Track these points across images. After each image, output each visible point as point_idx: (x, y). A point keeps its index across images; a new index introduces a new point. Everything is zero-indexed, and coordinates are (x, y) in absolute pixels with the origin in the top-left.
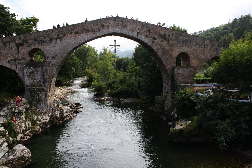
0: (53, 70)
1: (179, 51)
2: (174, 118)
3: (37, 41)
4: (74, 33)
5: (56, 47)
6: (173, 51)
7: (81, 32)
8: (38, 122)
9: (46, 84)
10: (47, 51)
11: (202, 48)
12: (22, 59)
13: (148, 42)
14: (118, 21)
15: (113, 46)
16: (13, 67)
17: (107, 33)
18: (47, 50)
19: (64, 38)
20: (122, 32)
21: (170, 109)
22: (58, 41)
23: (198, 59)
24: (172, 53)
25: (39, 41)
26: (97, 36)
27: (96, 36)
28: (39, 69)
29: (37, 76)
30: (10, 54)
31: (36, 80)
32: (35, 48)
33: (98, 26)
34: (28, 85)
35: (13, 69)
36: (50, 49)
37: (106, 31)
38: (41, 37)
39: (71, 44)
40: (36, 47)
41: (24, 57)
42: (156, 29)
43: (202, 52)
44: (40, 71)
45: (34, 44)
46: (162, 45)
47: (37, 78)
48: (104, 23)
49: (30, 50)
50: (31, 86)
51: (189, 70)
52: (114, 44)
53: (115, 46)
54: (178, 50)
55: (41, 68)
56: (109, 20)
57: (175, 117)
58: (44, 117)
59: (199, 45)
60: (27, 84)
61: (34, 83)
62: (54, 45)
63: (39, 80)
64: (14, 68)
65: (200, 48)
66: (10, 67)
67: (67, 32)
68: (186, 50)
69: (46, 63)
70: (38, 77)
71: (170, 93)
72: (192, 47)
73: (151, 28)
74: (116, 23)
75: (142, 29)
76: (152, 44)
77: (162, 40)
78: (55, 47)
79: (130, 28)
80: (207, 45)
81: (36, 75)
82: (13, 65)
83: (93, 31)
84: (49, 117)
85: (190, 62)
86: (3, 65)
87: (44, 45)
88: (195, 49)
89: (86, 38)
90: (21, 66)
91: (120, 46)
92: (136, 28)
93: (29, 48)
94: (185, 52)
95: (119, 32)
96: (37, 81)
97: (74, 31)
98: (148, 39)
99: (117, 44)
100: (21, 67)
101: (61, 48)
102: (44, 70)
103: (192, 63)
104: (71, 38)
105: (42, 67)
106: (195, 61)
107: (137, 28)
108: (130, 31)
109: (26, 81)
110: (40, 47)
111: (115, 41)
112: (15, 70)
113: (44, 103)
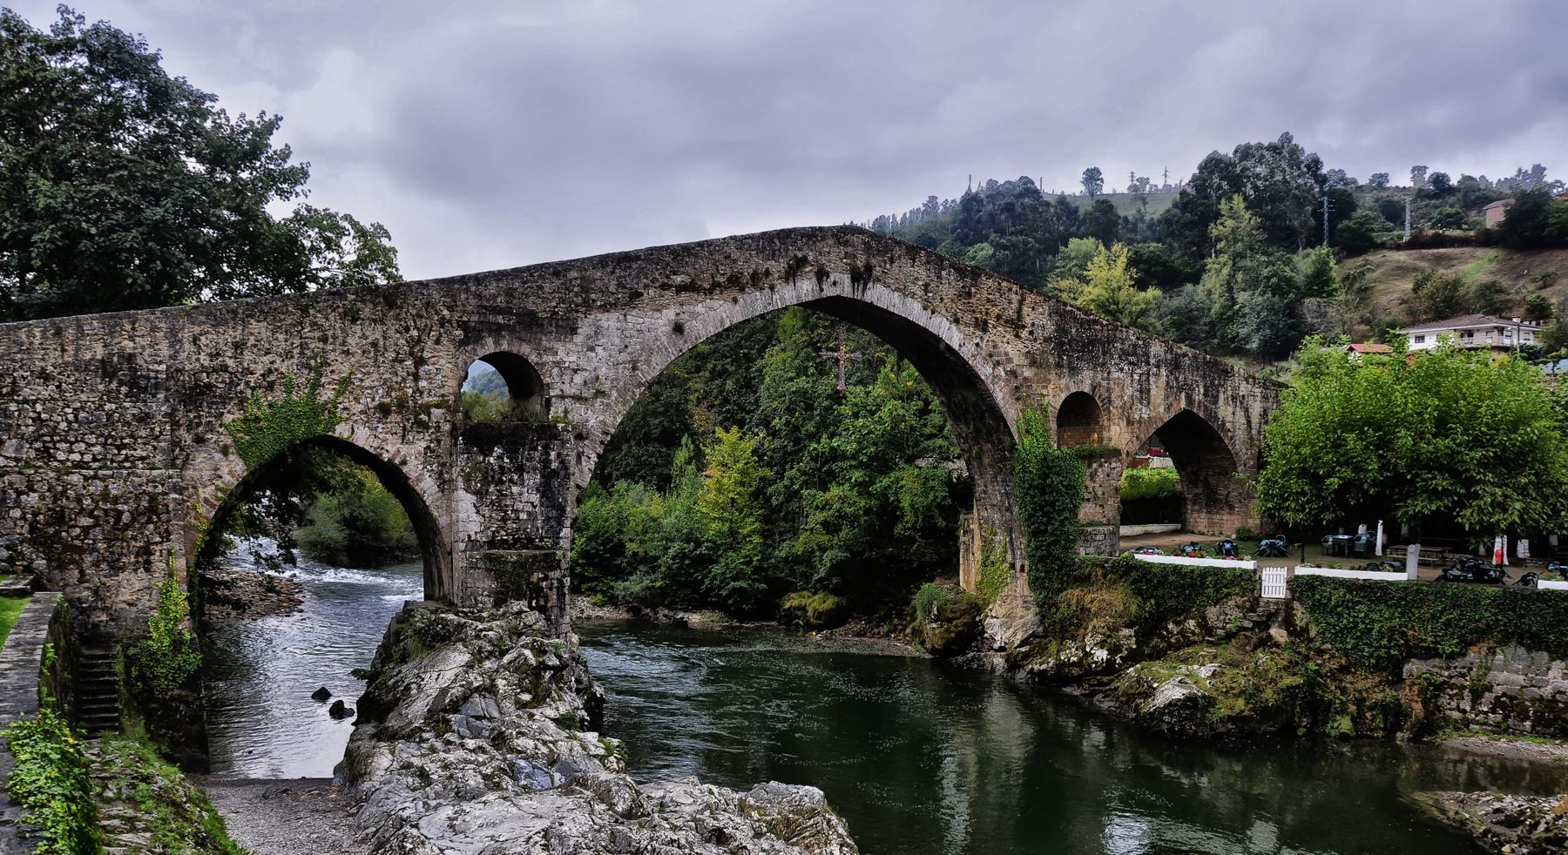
0: (584, 463)
2: (1089, 665)
4: (681, 289)
7: (707, 286)
10: (555, 371)
11: (1141, 375)
12: (437, 406)
14: (853, 246)
18: (557, 364)
21: (1033, 635)
22: (610, 321)
23: (1130, 422)
27: (765, 307)
28: (530, 459)
29: (521, 494)
30: (375, 376)
35: (386, 457)
36: (571, 359)
38: (527, 296)
40: (505, 347)
41: (443, 396)
43: (1141, 392)
44: (535, 469)
46: (1010, 360)
47: (519, 506)
48: (800, 250)
50: (492, 543)
54: (1063, 381)
55: (537, 454)
57: (1096, 663)
59: (1131, 363)
60: (469, 536)
61: (502, 528)
65: (1136, 377)
66: (375, 445)
68: (1088, 382)
69: (565, 429)
78: (592, 349)
80: (1158, 367)
83: (757, 280)
85: (1100, 433)
86: (337, 435)
92: (917, 279)
93: (469, 348)
94: (1086, 391)
96: (518, 518)
97: (678, 279)
100: (428, 448)
101: (624, 357)
102: (554, 465)
104: (665, 311)
105: (547, 449)
108: (896, 294)
110: (525, 349)
112: (397, 461)
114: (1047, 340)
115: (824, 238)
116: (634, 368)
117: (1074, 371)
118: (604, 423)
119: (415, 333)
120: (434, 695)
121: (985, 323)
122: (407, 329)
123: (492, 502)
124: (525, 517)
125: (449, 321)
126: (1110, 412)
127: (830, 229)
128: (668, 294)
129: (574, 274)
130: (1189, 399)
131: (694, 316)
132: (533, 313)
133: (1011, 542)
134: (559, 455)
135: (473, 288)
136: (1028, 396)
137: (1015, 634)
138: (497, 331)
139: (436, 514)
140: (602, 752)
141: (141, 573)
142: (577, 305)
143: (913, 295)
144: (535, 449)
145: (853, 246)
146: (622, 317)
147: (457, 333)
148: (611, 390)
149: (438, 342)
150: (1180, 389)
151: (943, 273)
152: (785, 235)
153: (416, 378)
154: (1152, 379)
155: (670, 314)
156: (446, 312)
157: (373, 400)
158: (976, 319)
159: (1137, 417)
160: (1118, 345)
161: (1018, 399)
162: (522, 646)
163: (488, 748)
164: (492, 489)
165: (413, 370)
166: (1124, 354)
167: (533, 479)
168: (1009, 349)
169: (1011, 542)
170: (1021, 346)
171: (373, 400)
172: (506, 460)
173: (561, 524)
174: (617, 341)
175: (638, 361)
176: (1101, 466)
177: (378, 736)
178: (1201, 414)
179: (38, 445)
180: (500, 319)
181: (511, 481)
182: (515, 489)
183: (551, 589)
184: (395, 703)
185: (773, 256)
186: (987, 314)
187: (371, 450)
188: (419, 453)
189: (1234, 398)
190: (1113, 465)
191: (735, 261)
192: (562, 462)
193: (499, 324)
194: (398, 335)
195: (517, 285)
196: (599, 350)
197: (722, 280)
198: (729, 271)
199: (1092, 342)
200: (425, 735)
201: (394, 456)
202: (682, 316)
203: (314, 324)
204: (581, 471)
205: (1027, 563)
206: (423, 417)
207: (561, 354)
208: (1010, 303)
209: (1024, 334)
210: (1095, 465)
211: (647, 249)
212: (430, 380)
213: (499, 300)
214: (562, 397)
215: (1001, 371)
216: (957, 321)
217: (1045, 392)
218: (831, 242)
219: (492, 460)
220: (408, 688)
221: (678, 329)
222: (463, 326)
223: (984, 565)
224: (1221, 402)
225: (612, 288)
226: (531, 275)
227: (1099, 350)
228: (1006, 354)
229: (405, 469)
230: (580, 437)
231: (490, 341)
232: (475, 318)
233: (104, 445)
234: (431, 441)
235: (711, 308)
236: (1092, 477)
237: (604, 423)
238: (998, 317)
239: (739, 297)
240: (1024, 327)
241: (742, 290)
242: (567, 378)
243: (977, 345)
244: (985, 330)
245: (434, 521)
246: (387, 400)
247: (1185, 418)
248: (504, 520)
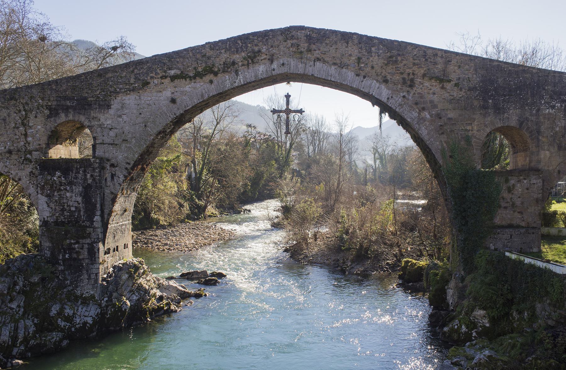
0: (116, 180)
4: (173, 78)
7: (191, 74)
8: (62, 323)
9: (95, 219)
10: (99, 129)
12: (36, 150)
13: (388, 98)
14: (298, 39)
15: (281, 114)
17: (265, 76)
19: (145, 91)
20: (310, 71)
22: (130, 100)
25: (77, 100)
26: (236, 85)
27: (232, 84)
32: (67, 120)
33: (238, 56)
34: (47, 221)
37: (261, 69)
39: (164, 108)
40: (71, 117)
41: (40, 145)
42: (415, 55)
46: (435, 106)
48: (256, 45)
49: (56, 124)
50: (56, 223)
51: (525, 181)
52: (284, 108)
53: (288, 111)
56: (271, 37)
58: (81, 310)
60: (44, 219)
62: (119, 113)
63: (76, 207)
67: (151, 75)
72: (538, 110)
73: (399, 55)
74: (292, 44)
75: (371, 59)
76: (400, 105)
77: (434, 89)
78: (120, 116)
79: (334, 57)
82: (12, 166)
84: (99, 310)
88: (549, 114)
89: (204, 91)
91: (301, 111)
92: (350, 55)
93: (52, 119)
95: (301, 71)
96: (70, 210)
97: (172, 72)
98: (388, 89)
99: (293, 107)
100: (32, 172)
102: (90, 181)
106: (547, 152)
107: (354, 58)
108: (333, 67)
109: (43, 208)
111: (288, 97)
113: (87, 271)
114: (470, 89)
115: (274, 36)
116: (145, 126)
117: (498, 110)
118: (127, 158)
119: (24, 113)
121: (412, 80)
122: (20, 111)
123: (56, 201)
124: (74, 209)
125: (42, 106)
126: (538, 140)
127: (280, 30)
128: (167, 81)
129: (110, 75)
131: (183, 93)
134: (92, 176)
135: (54, 87)
136: (452, 131)
138: (66, 109)
142: (110, 93)
143: (347, 66)
144: (79, 173)
145: (298, 39)
146: (138, 98)
147: (46, 112)
148: (132, 138)
149: (36, 117)
151: (373, 49)
152: (245, 38)
153: (26, 135)
155: (168, 94)
156: (40, 101)
157: (5, 148)
158: (404, 79)
161: (443, 133)
164: (56, 194)
165: (24, 132)
168: (435, 98)
170: (447, 95)
171: (5, 148)
173: (94, 215)
174: (135, 111)
175: (148, 122)
176: (519, 181)
180: (68, 103)
181: (66, 189)
182: (68, 194)
183: (82, 249)
185: (237, 51)
186: (413, 74)
188: (27, 175)
190: (535, 181)
191: (209, 58)
192: (94, 180)
193: (67, 106)
194: (15, 115)
195: (77, 84)
196: (124, 117)
197: (200, 69)
198: (204, 65)
201: (15, 176)
202: (176, 94)
204: (114, 185)
206: (28, 156)
207: (102, 120)
208: (435, 63)
209: (448, 86)
210: (512, 182)
211: (153, 56)
212: (33, 137)
213: (67, 93)
214: (103, 143)
215: (426, 115)
216: (386, 81)
217: (469, 128)
218: (281, 38)
219: (55, 178)
221: (173, 101)
222: (49, 108)
225: (132, 81)
226: (86, 78)
228: (431, 102)
230: (112, 165)
231: (63, 115)
235: (195, 88)
236: (510, 190)
237: (127, 158)
238: (424, 76)
239: (215, 79)
240: (449, 81)
241: (216, 74)
242: (104, 133)
243: (404, 97)
244: (411, 86)
246: (12, 148)
248: (63, 210)
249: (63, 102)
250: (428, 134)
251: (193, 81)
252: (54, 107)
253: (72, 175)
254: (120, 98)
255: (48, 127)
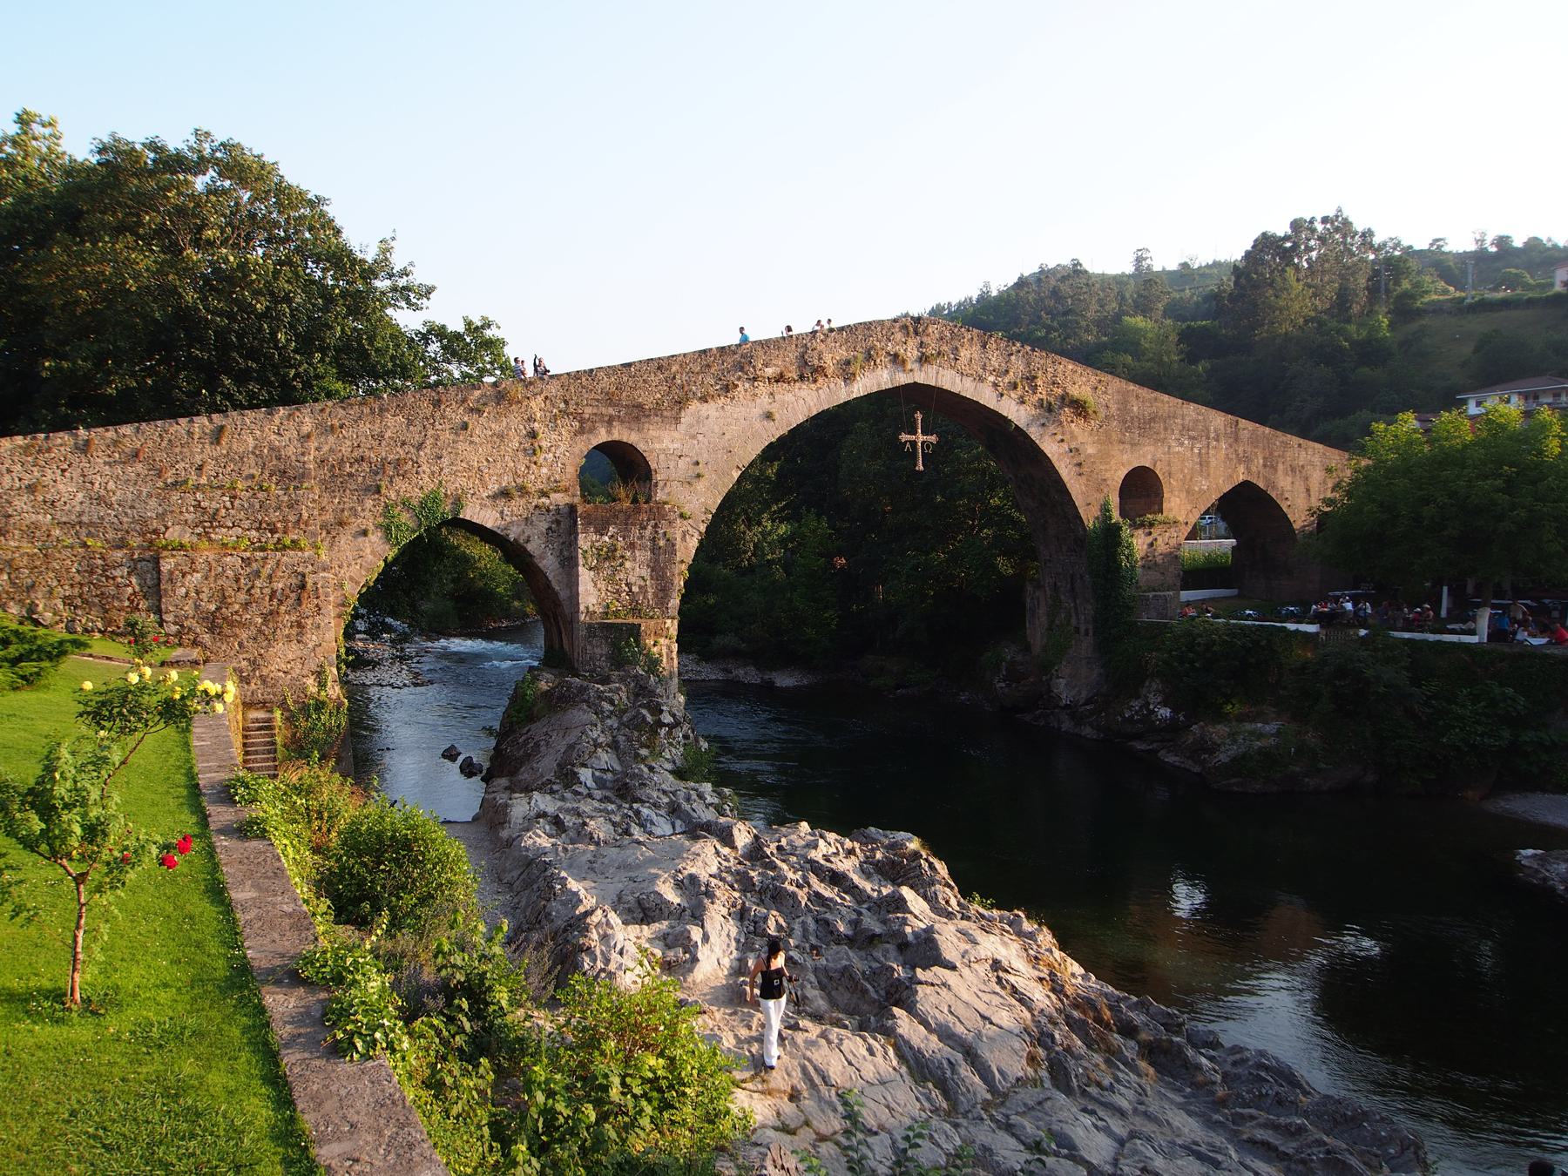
1: (1130, 463)
3: (622, 406)
5: (700, 437)
6: (1109, 463)
16: (514, 529)
17: (891, 386)
22: (709, 409)
24: (1106, 470)
31: (627, 585)
35: (512, 537)
36: (675, 446)
40: (616, 436)
45: (607, 419)
47: (632, 579)
54: (1125, 457)
57: (1159, 720)
59: (1191, 438)
60: (587, 608)
63: (640, 587)
64: (520, 529)
65: (1196, 451)
68: (1149, 457)
70: (636, 570)
71: (1087, 630)
78: (693, 437)
81: (628, 564)
86: (468, 518)
87: (651, 428)
88: (1178, 453)
90: (553, 523)
96: (631, 591)
97: (770, 371)
100: (550, 528)
103: (1171, 510)
105: (656, 526)
120: (562, 751)
130: (1248, 468)
132: (640, 406)
133: (1076, 608)
137: (1079, 693)
138: (610, 421)
139: (557, 588)
140: (716, 801)
141: (294, 645)
150: (1240, 461)
154: (1212, 452)
159: (1197, 489)
160: (1178, 421)
162: (640, 706)
163: (614, 798)
166: (1184, 429)
167: (643, 555)
169: (1076, 608)
172: (620, 539)
177: (511, 789)
178: (1261, 485)
179: (199, 530)
184: (528, 757)
187: (499, 532)
189: (1293, 469)
196: (700, 437)
199: (1153, 420)
200: (555, 787)
201: (519, 535)
203: (443, 417)
205: (1091, 627)
217: (1108, 467)
220: (537, 745)
221: (769, 416)
223: (1050, 629)
224: (1280, 472)
227: (1159, 426)
229: (529, 547)
231: (603, 431)
232: (588, 410)
233: (258, 529)
234: (553, 523)
245: (556, 594)
247: (1246, 485)
249: (604, 410)
250: (1069, 474)
251: (797, 384)
252: (587, 416)
253: (635, 531)
254: (694, 407)
255: (577, 450)
